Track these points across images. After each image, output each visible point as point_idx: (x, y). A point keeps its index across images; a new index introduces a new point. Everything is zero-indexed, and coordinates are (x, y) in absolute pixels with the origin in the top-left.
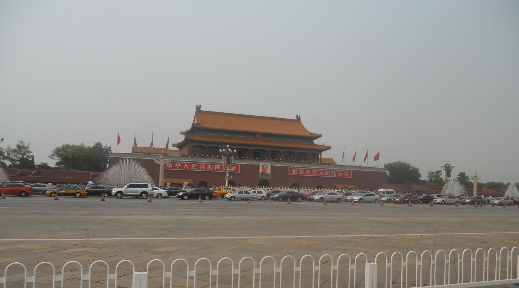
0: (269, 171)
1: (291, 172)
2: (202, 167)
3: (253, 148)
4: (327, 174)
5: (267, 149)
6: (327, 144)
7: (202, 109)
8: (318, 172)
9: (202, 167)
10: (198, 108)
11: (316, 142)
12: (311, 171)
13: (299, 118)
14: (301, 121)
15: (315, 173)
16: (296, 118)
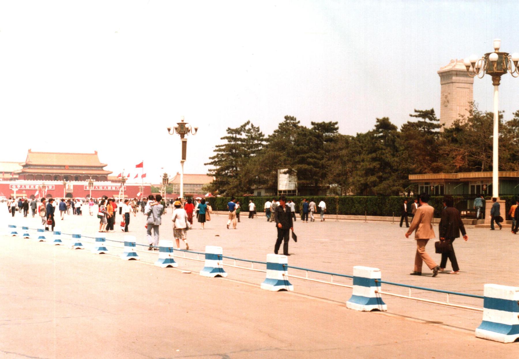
0: (72, 188)
1: (86, 188)
2: (32, 187)
3: (63, 175)
4: (109, 188)
5: (72, 175)
6: (111, 170)
7: (32, 151)
8: (103, 188)
9: (32, 187)
10: (30, 151)
11: (104, 168)
12: (98, 187)
13: (96, 153)
14: (98, 154)
15: (101, 189)
16: (94, 153)
